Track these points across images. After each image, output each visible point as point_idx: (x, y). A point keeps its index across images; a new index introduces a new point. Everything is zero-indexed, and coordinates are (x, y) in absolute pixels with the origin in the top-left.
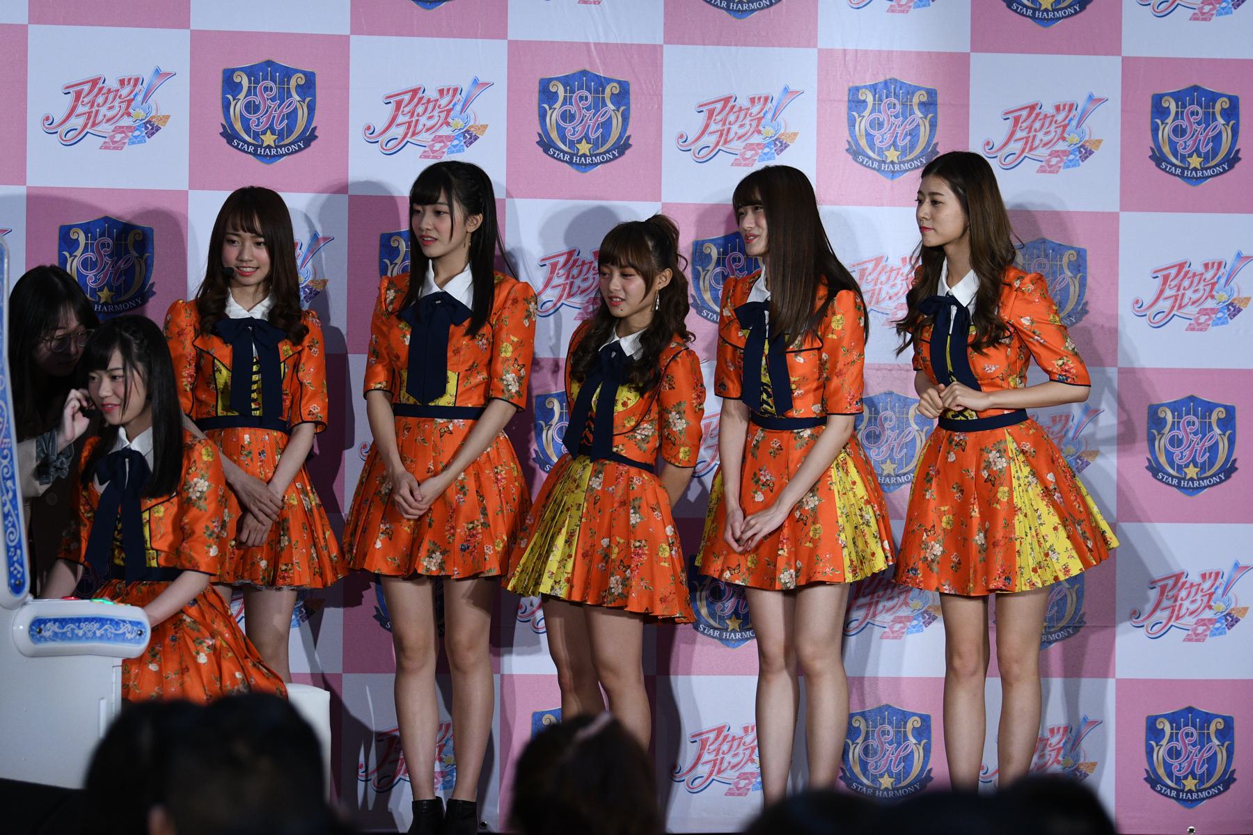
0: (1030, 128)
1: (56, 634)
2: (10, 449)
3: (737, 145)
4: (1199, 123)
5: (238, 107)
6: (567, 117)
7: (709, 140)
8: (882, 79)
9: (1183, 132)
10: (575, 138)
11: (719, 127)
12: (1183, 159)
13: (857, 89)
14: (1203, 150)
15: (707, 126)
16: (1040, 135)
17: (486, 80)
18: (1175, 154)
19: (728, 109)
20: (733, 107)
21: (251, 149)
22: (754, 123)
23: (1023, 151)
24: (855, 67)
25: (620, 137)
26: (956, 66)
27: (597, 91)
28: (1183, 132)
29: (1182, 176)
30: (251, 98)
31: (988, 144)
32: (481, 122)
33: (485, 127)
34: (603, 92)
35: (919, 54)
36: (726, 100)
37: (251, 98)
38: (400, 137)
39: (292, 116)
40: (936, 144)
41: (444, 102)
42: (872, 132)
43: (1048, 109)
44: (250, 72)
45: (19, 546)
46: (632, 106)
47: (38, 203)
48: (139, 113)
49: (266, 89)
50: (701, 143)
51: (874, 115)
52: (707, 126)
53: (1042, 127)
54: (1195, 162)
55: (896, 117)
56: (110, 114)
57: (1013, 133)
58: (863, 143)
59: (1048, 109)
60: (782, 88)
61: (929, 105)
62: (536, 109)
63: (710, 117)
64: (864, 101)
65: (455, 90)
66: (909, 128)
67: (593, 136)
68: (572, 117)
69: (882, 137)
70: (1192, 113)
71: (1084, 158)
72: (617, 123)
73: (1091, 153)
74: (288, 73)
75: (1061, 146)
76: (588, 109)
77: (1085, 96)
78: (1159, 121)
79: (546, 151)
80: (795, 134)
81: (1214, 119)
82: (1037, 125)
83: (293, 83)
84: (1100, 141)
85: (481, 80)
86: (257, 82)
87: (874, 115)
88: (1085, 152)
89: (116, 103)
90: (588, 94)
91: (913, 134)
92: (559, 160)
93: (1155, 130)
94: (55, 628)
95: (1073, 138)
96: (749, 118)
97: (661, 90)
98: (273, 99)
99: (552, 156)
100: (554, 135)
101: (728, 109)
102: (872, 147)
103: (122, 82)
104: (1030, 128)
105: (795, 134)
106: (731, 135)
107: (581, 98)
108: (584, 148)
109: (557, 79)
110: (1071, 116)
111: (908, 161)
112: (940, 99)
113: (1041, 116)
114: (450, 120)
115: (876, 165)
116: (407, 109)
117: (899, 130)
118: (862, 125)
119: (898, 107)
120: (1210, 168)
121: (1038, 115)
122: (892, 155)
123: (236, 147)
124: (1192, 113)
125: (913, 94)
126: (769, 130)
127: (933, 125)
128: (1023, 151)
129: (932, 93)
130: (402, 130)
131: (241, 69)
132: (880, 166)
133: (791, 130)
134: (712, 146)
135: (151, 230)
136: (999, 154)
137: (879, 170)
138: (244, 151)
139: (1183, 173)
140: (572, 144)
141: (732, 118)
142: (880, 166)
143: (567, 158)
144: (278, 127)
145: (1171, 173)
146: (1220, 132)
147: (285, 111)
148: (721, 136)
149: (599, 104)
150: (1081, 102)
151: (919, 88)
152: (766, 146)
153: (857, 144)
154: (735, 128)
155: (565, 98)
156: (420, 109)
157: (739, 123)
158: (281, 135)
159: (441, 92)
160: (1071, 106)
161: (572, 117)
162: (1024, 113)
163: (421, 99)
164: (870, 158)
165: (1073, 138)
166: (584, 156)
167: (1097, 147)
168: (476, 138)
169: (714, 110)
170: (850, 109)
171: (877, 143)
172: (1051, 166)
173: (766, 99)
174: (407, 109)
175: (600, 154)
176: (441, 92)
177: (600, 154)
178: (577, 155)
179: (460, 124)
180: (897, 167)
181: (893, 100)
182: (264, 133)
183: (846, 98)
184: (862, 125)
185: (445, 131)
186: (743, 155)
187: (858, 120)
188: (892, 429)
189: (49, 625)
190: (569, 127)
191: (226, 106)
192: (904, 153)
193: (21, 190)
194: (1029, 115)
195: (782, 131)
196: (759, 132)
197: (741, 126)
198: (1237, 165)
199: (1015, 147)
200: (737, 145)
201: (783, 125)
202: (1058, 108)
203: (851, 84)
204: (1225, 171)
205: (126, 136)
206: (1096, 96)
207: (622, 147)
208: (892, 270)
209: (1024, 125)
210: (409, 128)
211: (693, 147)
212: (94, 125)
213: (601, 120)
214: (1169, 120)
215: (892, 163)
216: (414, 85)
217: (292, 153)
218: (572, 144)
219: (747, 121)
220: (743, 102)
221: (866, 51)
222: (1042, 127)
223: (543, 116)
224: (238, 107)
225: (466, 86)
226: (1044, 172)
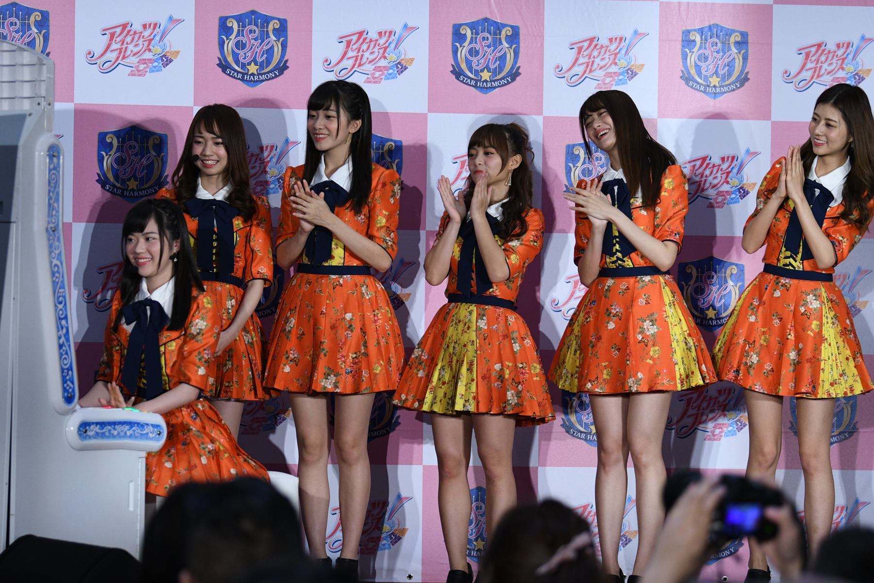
0: (817, 61)
1: (97, 433)
2: (64, 297)
3: (599, 74)
5: (230, 45)
6: (473, 52)
7: (579, 70)
8: (707, 24)
10: (479, 68)
11: (586, 60)
13: (689, 32)
15: (577, 59)
16: (825, 66)
17: (414, 25)
19: (592, 46)
20: (596, 45)
21: (240, 76)
22: (612, 57)
23: (812, 78)
24: (687, 15)
25: (512, 68)
26: (764, 14)
27: (495, 34)
30: (240, 38)
31: (786, 72)
32: (409, 56)
33: (413, 60)
34: (500, 34)
35: (735, 5)
36: (592, 40)
37: (240, 38)
38: (349, 68)
39: (270, 52)
41: (382, 41)
42: (700, 64)
43: (831, 46)
44: (239, 19)
45: (70, 368)
46: (521, 45)
47: (83, 115)
48: (157, 49)
49: (251, 31)
50: (572, 72)
52: (577, 59)
55: (718, 52)
56: (136, 50)
58: (693, 72)
59: (831, 46)
60: (632, 31)
61: (742, 43)
62: (450, 47)
63: (579, 53)
65: (391, 33)
66: (727, 61)
67: (492, 67)
68: (477, 53)
69: (707, 67)
72: (510, 57)
74: (267, 20)
76: (489, 47)
77: (859, 36)
79: (457, 78)
80: (643, 66)
82: (823, 58)
83: (271, 27)
84: (869, 71)
85: (410, 25)
86: (244, 26)
89: (140, 42)
91: (730, 65)
94: (97, 429)
96: (608, 53)
98: (256, 39)
99: (462, 82)
100: (464, 66)
101: (592, 46)
102: (699, 74)
103: (145, 26)
104: (817, 61)
105: (643, 66)
106: (595, 66)
107: (484, 39)
108: (486, 75)
109: (465, 24)
110: (848, 51)
111: (727, 85)
112: (750, 41)
113: (826, 52)
114: (386, 55)
115: (702, 88)
116: (355, 47)
117: (720, 62)
118: (692, 59)
121: (824, 50)
122: (715, 81)
123: (229, 75)
125: (730, 35)
126: (622, 63)
127: (745, 58)
128: (812, 78)
129: (744, 35)
130: (351, 61)
131: (233, 17)
132: (705, 89)
133: (639, 62)
134: (581, 74)
135: (166, 136)
136: (794, 80)
137: (705, 92)
138: (234, 77)
140: (477, 73)
141: (595, 53)
142: (705, 89)
143: (473, 83)
144: (259, 60)
147: (265, 48)
148: (588, 66)
149: (497, 42)
150: (856, 41)
151: (734, 31)
152: (620, 74)
153: (689, 73)
154: (597, 61)
156: (364, 47)
157: (600, 57)
158: (262, 66)
159: (380, 34)
160: (849, 44)
161: (477, 53)
162: (813, 49)
163: (365, 39)
164: (698, 83)
166: (486, 81)
167: (868, 74)
170: (683, 46)
171: (704, 72)
173: (621, 39)
174: (355, 47)
176: (380, 34)
179: (394, 58)
180: (718, 90)
181: (715, 40)
182: (249, 64)
183: (680, 39)
184: (692, 59)
185: (383, 63)
186: (603, 80)
187: (689, 55)
189: (92, 427)
190: (474, 60)
191: (221, 44)
192: (723, 79)
193: (70, 106)
194: (817, 51)
195: (633, 63)
196: (616, 64)
197: (602, 59)
200: (599, 74)
201: (633, 58)
202: (838, 46)
203: (684, 28)
205: (148, 67)
206: (867, 36)
207: (514, 75)
209: (813, 58)
210: (356, 61)
211: (566, 75)
212: (124, 58)
213: (498, 55)
215: (715, 86)
216: (360, 29)
217: (270, 79)
218: (477, 73)
219: (607, 56)
220: (604, 41)
221: (695, 3)
223: (455, 52)
224: (230, 45)
225: (398, 29)
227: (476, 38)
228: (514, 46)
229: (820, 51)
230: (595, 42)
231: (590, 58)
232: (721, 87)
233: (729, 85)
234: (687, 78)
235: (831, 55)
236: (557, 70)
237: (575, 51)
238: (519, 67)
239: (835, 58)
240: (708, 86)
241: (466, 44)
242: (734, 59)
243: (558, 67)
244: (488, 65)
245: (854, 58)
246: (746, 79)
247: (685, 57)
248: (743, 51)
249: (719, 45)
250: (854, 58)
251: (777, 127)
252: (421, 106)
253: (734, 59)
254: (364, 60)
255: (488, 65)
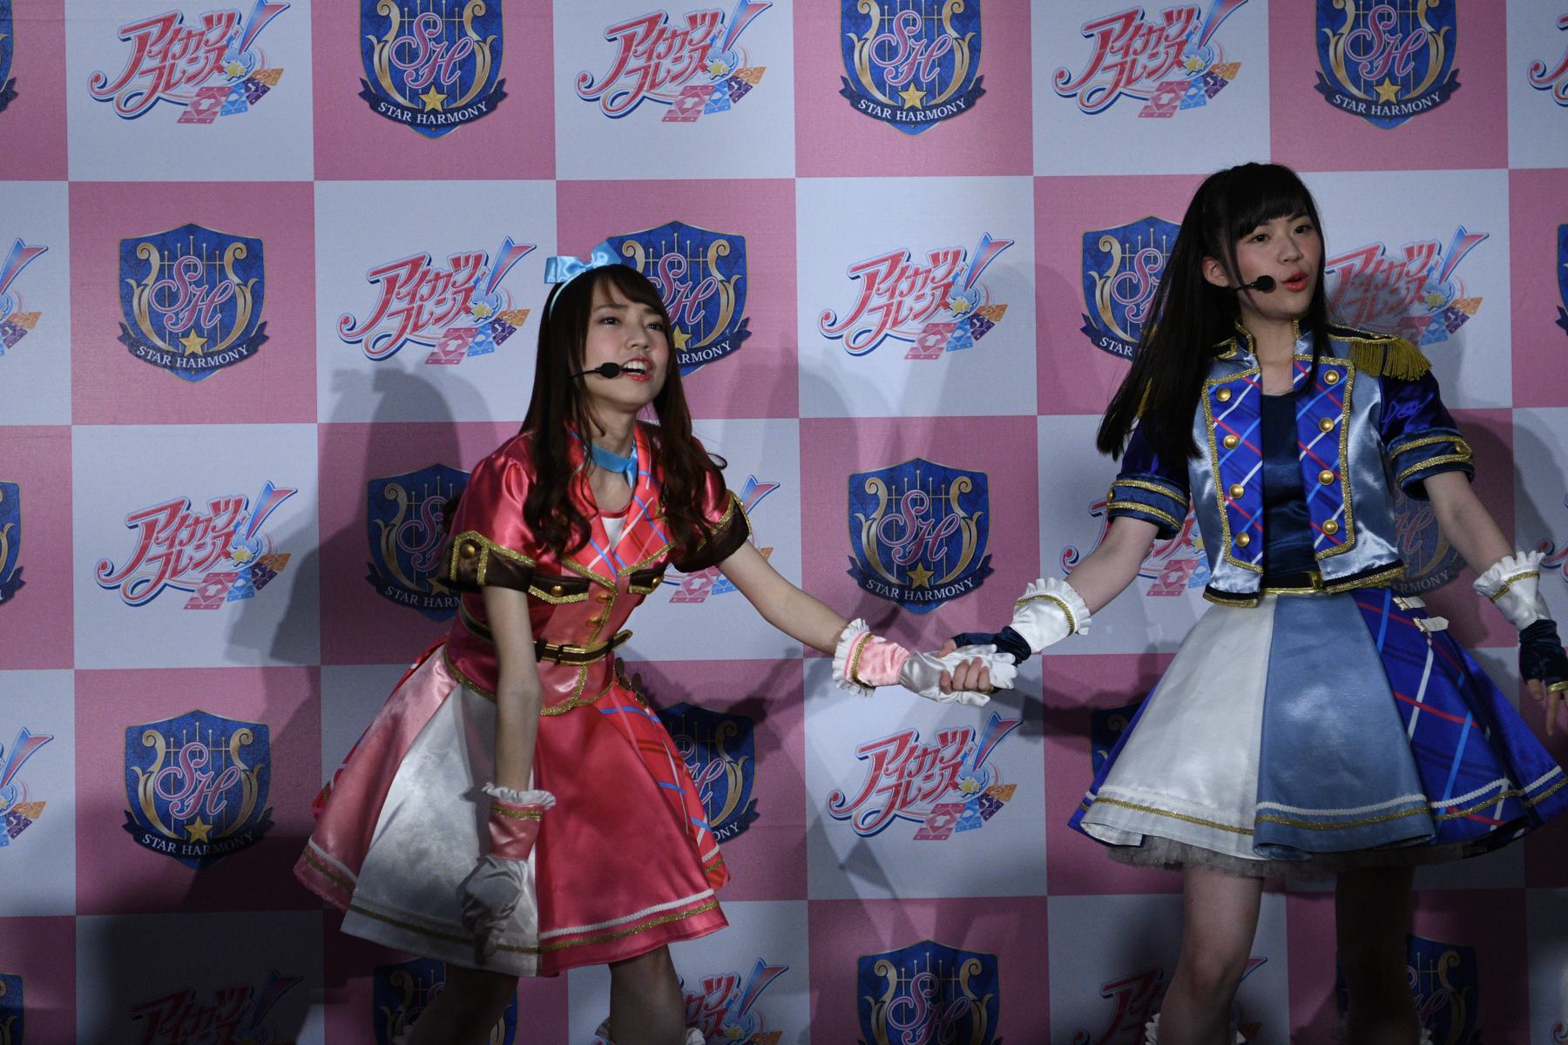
0: (1126, 50)
3: (671, 90)
4: (1392, 32)
7: (628, 82)
9: (1368, 47)
11: (641, 62)
12: (1369, 87)
14: (1400, 74)
15: (622, 62)
16: (1142, 59)
18: (1355, 80)
19: (655, 34)
20: (663, 31)
23: (1116, 85)
27: (450, 14)
28: (1368, 47)
29: (1366, 114)
32: (272, 65)
33: (279, 72)
34: (461, 16)
36: (653, 21)
38: (146, 92)
40: (981, 79)
41: (213, 35)
51: (882, 37)
52: (622, 62)
53: (1145, 48)
54: (1388, 92)
57: (1099, 58)
58: (867, 80)
63: (627, 48)
64: (867, 16)
66: (937, 54)
67: (446, 82)
68: (413, 56)
70: (1381, 17)
71: (1212, 92)
73: (1223, 83)
75: (1176, 75)
76: (438, 40)
78: (1328, 31)
80: (761, 70)
81: (1417, 25)
82: (1138, 44)
84: (1236, 66)
87: (882, 37)
88: (1214, 83)
90: (436, 17)
91: (946, 62)
92: (396, 119)
93: (1323, 45)
95: (1194, 61)
96: (687, 48)
97: (550, 7)
99: (384, 114)
100: (386, 82)
101: (655, 34)
102: (880, 85)
105: (761, 70)
107: (427, 25)
108: (433, 100)
110: (1190, 27)
111: (937, 106)
113: (1144, 30)
114: (223, 63)
116: (156, 49)
118: (865, 52)
119: (919, 22)
120: (1411, 100)
121: (1138, 28)
122: (913, 97)
124: (1381, 17)
126: (719, 65)
127: (975, 49)
128: (1116, 85)
132: (894, 115)
133: (754, 63)
134: (632, 91)
136: (1079, 91)
139: (1368, 109)
140: (414, 95)
141: (661, 48)
142: (894, 115)
143: (407, 116)
145: (1351, 111)
146: (1426, 45)
149: (454, 32)
153: (857, 81)
155: (402, 24)
156: (177, 48)
162: (1117, 26)
165: (1194, 61)
166: (434, 112)
168: (265, 90)
169: (634, 35)
172: (1160, 107)
173: (714, 16)
174: (156, 49)
175: (458, 109)
176: (208, 20)
177: (458, 109)
178: (422, 111)
183: (838, 12)
184: (865, 52)
187: (858, 46)
188: (925, 518)
190: (408, 68)
192: (931, 93)
195: (740, 65)
196: (704, 68)
197: (676, 60)
198: (1453, 95)
199: (1104, 78)
200: (671, 90)
201: (741, 56)
202: (1169, 16)
204: (1435, 105)
207: (493, 97)
208: (917, 273)
211: (602, 95)
214: (1345, 29)
218: (414, 95)
219: (685, 52)
220: (678, 23)
222: (1145, 48)
223: (367, 52)
226: (1151, 115)
227: (410, 23)
228: (490, 39)
229: (1131, 30)
230: (661, 25)
231: (650, 58)
232: (924, 109)
233: (944, 104)
234: (854, 94)
235: (1154, 37)
236: (583, 85)
237: (617, 46)
238: (502, 82)
239: (1164, 44)
240: (901, 109)
241: (390, 36)
242: (952, 51)
243: (584, 79)
244: (437, 79)
245: (1203, 41)
246: (979, 92)
247: (848, 49)
248: (970, 35)
249: (919, 22)
250: (1203, 41)
251: (1047, 190)
252: (298, 165)
253: (952, 51)
254: (177, 75)
255: (437, 79)
